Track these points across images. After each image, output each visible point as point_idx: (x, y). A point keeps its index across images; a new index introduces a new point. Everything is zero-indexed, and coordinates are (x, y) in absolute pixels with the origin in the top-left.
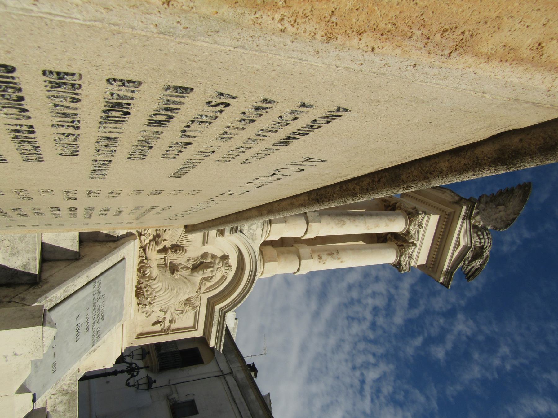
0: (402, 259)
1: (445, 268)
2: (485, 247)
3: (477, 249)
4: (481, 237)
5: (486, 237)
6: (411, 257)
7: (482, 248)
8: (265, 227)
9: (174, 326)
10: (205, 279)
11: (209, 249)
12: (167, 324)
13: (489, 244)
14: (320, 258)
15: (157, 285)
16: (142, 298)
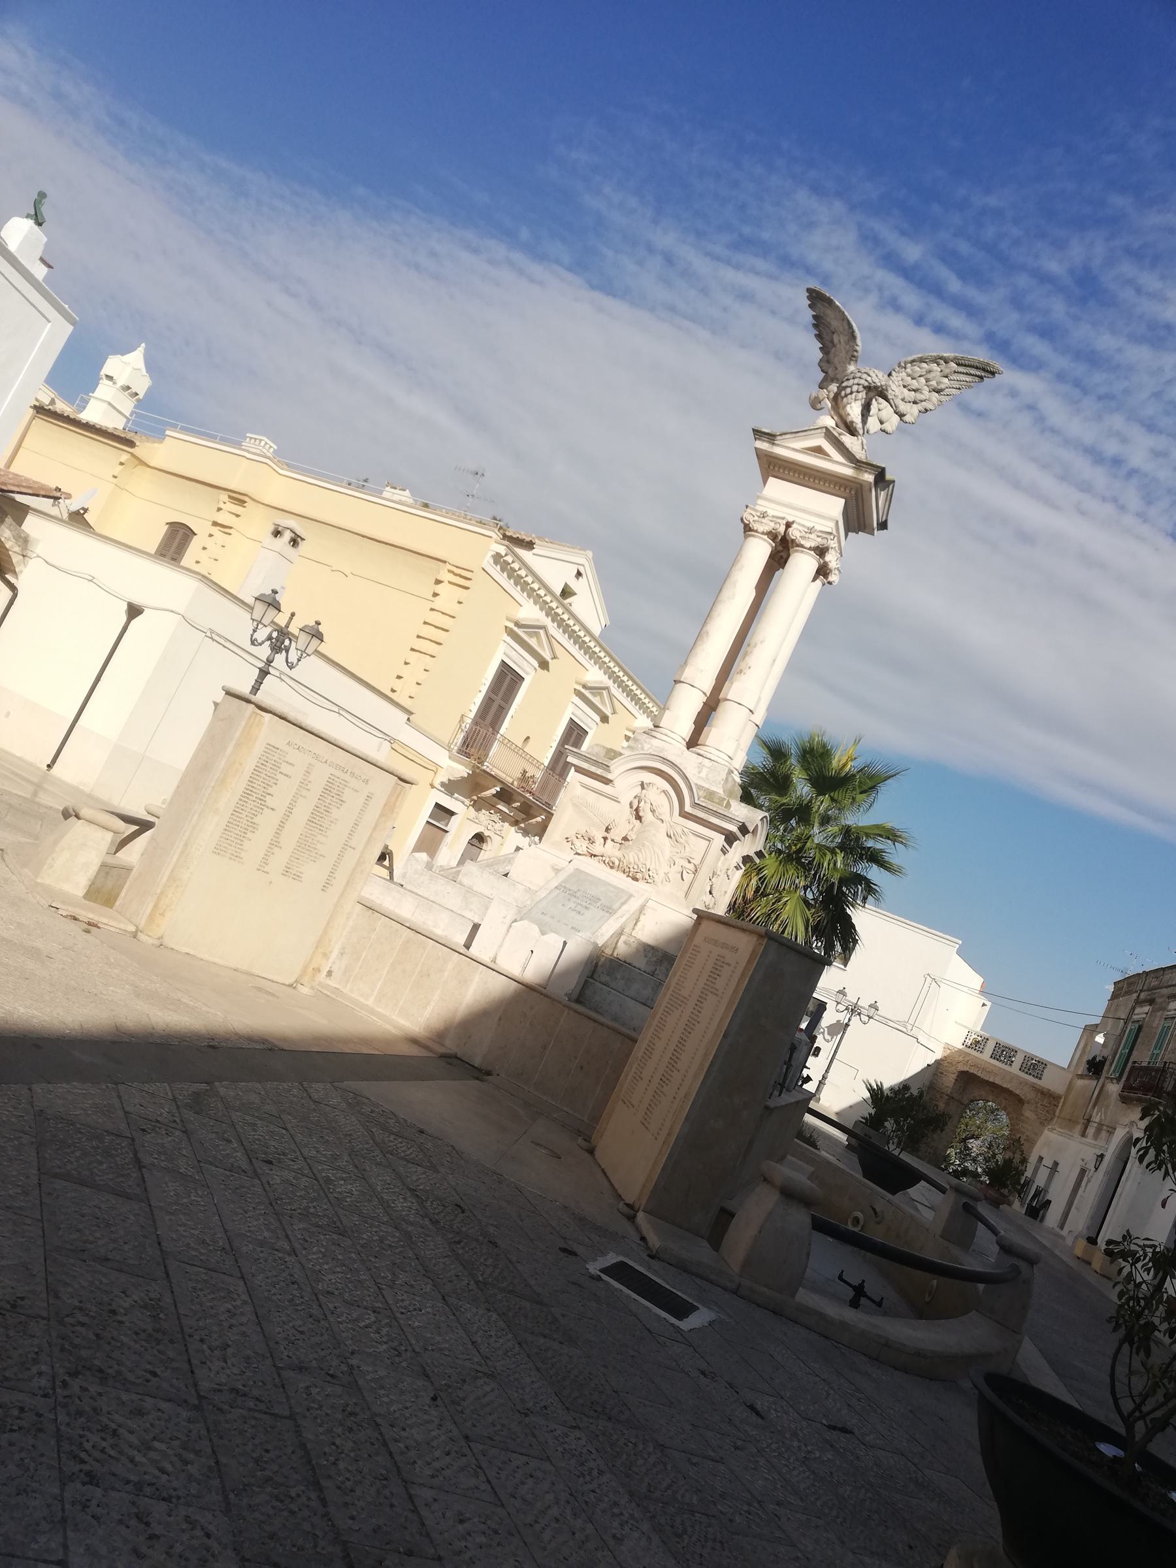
0: (808, 545)
1: (847, 471)
2: (866, 384)
3: (871, 394)
4: (848, 390)
5: (851, 382)
6: (811, 530)
7: (868, 389)
8: (658, 735)
9: (697, 862)
10: (653, 811)
11: (627, 797)
12: (691, 867)
13: (865, 376)
14: (741, 671)
15: (631, 857)
16: (639, 876)
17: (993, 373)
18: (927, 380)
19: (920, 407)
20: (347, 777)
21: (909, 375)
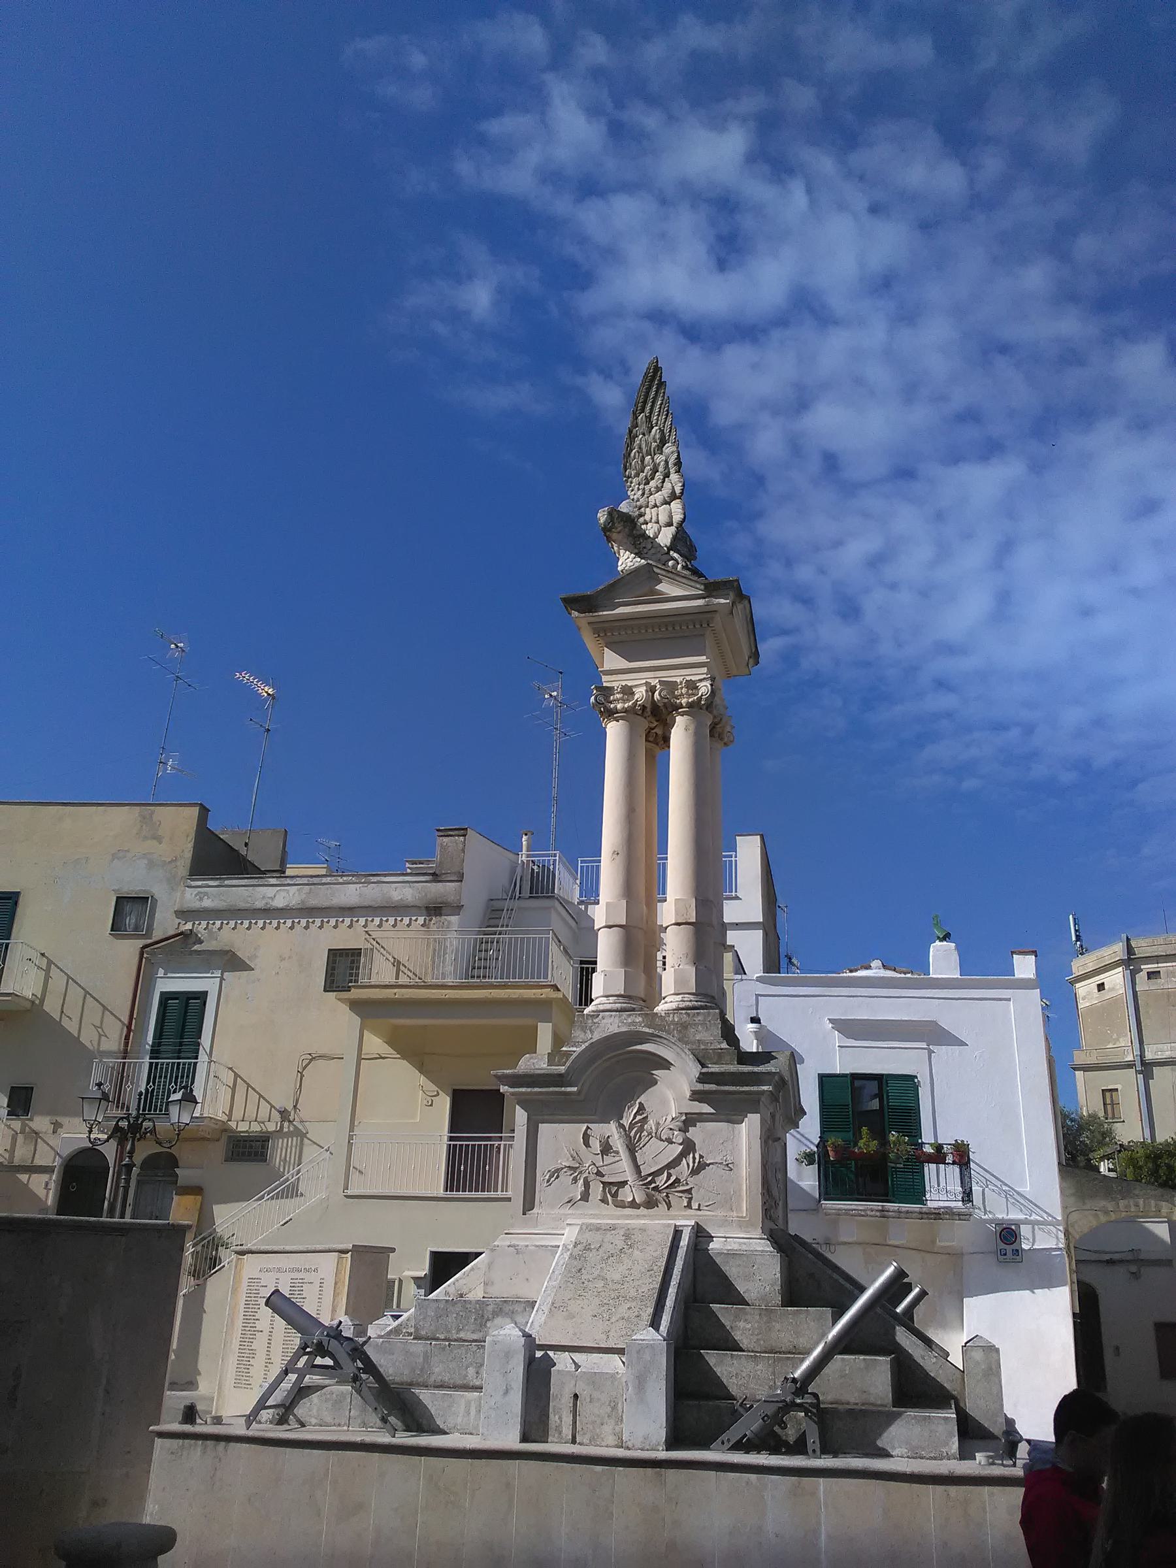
17: (657, 369)
18: (649, 453)
19: (672, 471)
20: (300, 1275)
21: (637, 475)
